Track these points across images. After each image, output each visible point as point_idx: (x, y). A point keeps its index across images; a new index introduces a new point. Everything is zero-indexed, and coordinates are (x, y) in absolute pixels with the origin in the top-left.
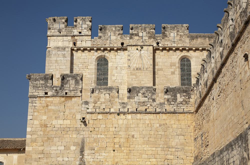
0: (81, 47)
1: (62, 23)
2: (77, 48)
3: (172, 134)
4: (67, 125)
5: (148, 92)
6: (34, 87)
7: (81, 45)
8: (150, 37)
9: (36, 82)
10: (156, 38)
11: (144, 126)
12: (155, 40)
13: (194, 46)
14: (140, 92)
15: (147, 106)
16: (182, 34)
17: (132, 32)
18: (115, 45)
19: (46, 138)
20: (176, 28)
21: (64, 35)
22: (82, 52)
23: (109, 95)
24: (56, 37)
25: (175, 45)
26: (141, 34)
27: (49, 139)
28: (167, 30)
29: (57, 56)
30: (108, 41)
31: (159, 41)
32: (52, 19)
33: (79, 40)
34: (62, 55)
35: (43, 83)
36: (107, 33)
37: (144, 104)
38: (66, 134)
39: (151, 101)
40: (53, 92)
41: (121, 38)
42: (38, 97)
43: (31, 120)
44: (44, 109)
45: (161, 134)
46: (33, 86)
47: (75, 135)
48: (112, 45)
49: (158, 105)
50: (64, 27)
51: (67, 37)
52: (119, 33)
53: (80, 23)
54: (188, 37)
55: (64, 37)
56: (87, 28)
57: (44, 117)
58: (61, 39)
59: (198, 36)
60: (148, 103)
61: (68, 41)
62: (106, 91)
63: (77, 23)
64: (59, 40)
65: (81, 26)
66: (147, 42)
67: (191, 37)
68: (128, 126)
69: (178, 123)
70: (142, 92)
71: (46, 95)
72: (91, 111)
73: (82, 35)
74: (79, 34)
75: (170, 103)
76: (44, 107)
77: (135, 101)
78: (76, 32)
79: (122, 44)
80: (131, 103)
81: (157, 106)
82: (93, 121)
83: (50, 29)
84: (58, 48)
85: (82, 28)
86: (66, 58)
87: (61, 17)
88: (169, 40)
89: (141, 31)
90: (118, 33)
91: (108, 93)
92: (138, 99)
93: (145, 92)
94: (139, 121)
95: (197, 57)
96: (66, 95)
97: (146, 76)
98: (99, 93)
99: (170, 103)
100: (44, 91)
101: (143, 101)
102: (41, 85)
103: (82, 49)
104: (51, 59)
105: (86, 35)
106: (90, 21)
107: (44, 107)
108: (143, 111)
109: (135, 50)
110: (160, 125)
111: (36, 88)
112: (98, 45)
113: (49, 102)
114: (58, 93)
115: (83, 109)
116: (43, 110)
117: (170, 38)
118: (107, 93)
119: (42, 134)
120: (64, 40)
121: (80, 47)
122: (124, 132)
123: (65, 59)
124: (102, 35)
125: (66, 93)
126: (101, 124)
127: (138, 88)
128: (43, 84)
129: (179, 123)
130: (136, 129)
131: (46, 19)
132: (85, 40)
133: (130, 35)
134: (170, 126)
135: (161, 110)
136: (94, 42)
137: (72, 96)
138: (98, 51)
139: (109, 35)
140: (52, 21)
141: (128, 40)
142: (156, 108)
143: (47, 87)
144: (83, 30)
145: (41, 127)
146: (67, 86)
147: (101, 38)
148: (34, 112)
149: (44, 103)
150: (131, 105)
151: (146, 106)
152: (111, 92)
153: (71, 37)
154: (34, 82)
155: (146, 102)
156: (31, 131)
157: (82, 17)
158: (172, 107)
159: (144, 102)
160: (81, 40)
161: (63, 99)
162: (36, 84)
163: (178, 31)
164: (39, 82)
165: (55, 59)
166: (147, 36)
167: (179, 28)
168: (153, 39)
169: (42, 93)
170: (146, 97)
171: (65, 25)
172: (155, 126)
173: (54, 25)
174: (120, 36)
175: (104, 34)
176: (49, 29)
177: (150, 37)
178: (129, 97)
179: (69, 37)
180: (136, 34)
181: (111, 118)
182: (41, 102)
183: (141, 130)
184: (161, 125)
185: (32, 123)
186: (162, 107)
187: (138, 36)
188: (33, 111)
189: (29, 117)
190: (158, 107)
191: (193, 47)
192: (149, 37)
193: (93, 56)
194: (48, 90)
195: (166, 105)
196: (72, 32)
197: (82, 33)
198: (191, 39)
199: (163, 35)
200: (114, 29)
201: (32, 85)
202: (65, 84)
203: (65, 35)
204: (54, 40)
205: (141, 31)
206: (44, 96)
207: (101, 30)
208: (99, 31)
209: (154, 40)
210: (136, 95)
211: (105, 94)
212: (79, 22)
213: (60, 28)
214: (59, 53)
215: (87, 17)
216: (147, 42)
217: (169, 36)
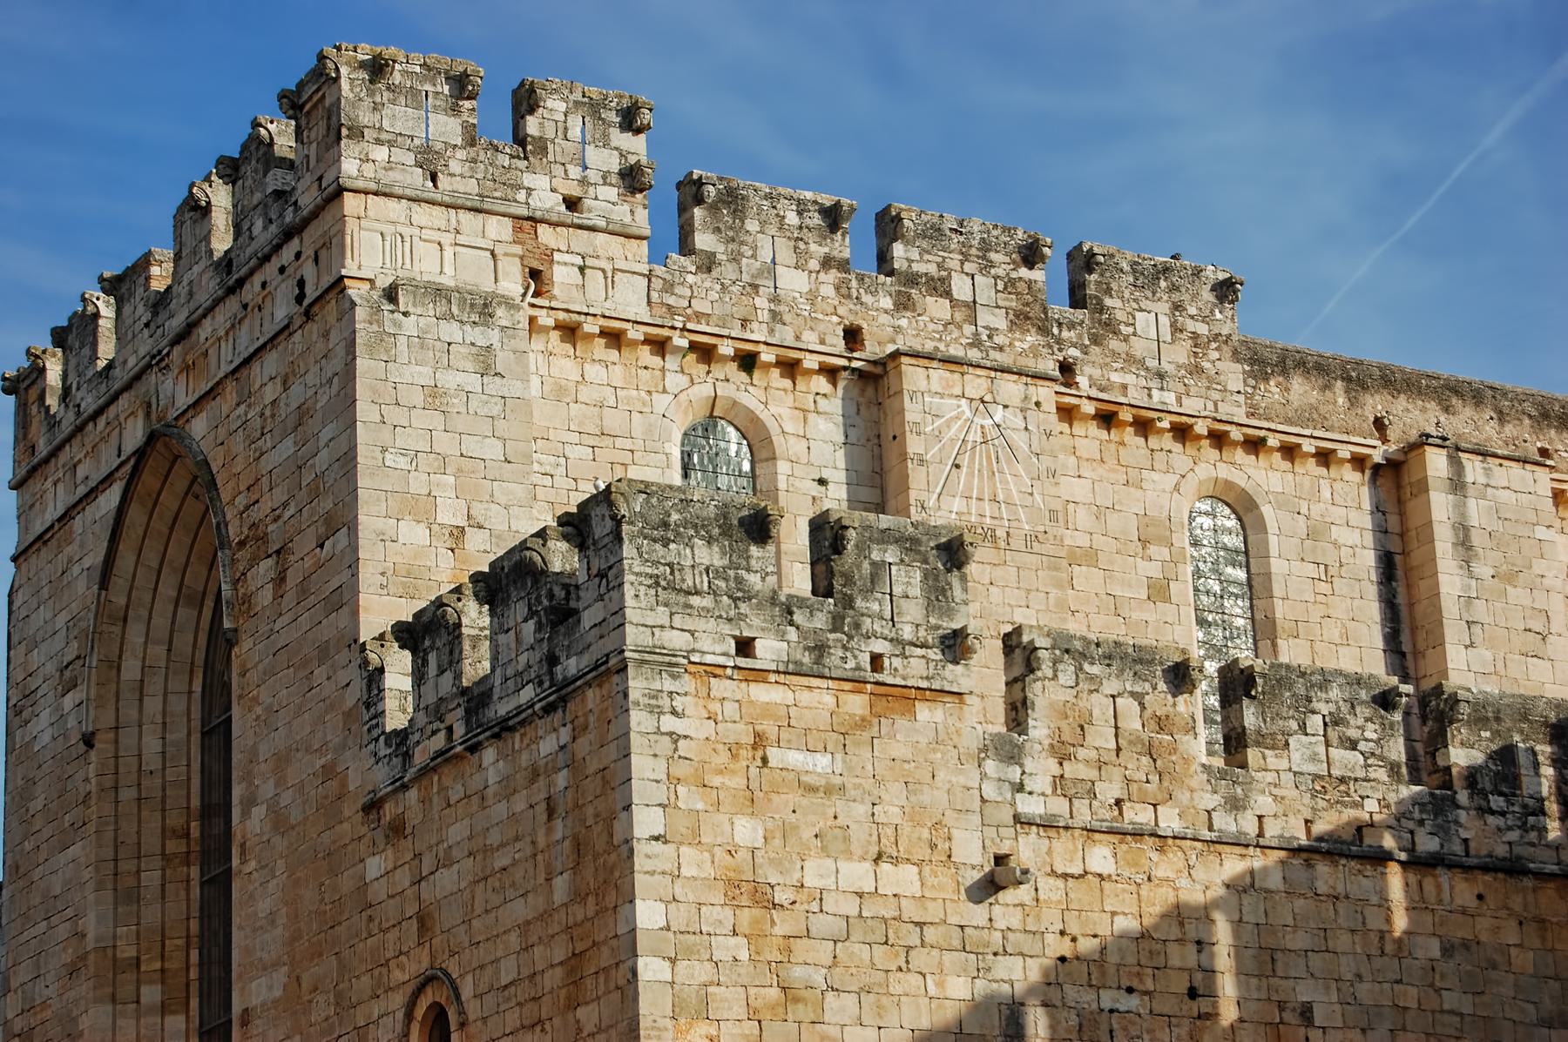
3: (1516, 1016)
4: (904, 902)
5: (1358, 709)
6: (657, 584)
7: (576, 294)
8: (1020, 319)
9: (666, 546)
10: (1055, 331)
11: (1359, 951)
12: (1051, 347)
13: (1273, 426)
14: (1316, 705)
15: (1362, 806)
16: (1202, 329)
17: (910, 261)
18: (804, 338)
19: (774, 993)
20: (1163, 284)
21: (460, 202)
23: (1142, 706)
25: (1170, 398)
26: (961, 288)
27: (796, 1000)
28: (1114, 286)
30: (761, 302)
31: (1075, 359)
34: (474, 351)
35: (718, 562)
36: (750, 239)
37: (1348, 795)
38: (900, 969)
39: (1382, 774)
40: (788, 637)
41: (844, 291)
42: (692, 668)
43: (657, 839)
44: (738, 766)
45: (1455, 1006)
46: (650, 582)
47: (962, 979)
48: (786, 335)
49: (1421, 812)
50: (459, 141)
52: (826, 250)
53: (566, 129)
54: (1236, 356)
55: (465, 216)
57: (747, 831)
59: (1289, 362)
60: (1365, 788)
62: (1117, 676)
66: (1001, 349)
67: (1252, 361)
68: (1270, 942)
69: (1537, 943)
70: (1325, 709)
71: (742, 662)
72: (1042, 811)
74: (563, 208)
75: (1484, 803)
76: (733, 750)
77: (1295, 769)
78: (543, 193)
79: (853, 336)
80: (1270, 777)
81: (1417, 815)
82: (1060, 883)
83: (357, 133)
88: (1131, 360)
89: (962, 264)
90: (818, 250)
91: (1133, 694)
92: (1308, 752)
93: (1345, 708)
94: (1332, 912)
95: (1281, 503)
96: (879, 677)
97: (1029, 591)
98: (1077, 684)
99: (1484, 803)
100: (727, 629)
101: (1336, 772)
105: (617, 228)
107: (733, 750)
108: (1343, 842)
109: (951, 396)
110: (1448, 951)
111: (673, 597)
112: (699, 316)
113: (767, 710)
114: (820, 650)
115: (990, 791)
116: (733, 772)
117: (1139, 347)
118: (1129, 688)
119: (744, 955)
122: (1254, 981)
123: (494, 384)
124: (720, 248)
125: (876, 661)
126: (1114, 914)
127: (1303, 674)
128: (721, 574)
129: (1543, 939)
130: (1316, 961)
133: (900, 283)
134: (1498, 957)
135: (1442, 846)
137: (919, 688)
139: (765, 255)
141: (886, 312)
142: (1411, 825)
143: (750, 599)
144: (591, 189)
145: (732, 902)
146: (876, 607)
147: (714, 273)
148: (673, 780)
149: (738, 719)
150: (1275, 791)
151: (1355, 805)
152: (1147, 686)
153: (508, 222)
154: (658, 546)
155: (1356, 780)
156: (668, 929)
158: (1499, 829)
159: (1342, 780)
161: (857, 704)
162: (670, 565)
163: (1177, 307)
164: (688, 551)
165: (423, 374)
166: (998, 307)
167: (1183, 290)
168: (1039, 337)
169: (715, 645)
170: (1353, 745)
172: (1419, 953)
174: (833, 275)
175: (734, 241)
177: (1020, 319)
178: (1258, 732)
180: (932, 279)
181: (1172, 875)
182: (715, 707)
183: (1347, 969)
184: (1452, 946)
185: (668, 867)
186: (1446, 825)
187: (947, 294)
188: (664, 777)
189: (646, 821)
190: (1421, 823)
191: (1269, 430)
192: (1011, 316)
193: (655, 395)
194: (756, 622)
195: (1463, 814)
196: (519, 187)
197: (590, 211)
198: (1251, 375)
199: (1092, 319)
200: (792, 218)
202: (868, 592)
203: (469, 204)
205: (962, 264)
206: (735, 667)
209: (1041, 340)
210: (1294, 725)
211: (1113, 697)
213: (427, 138)
214: (450, 331)
216: (1001, 349)
217: (1131, 330)
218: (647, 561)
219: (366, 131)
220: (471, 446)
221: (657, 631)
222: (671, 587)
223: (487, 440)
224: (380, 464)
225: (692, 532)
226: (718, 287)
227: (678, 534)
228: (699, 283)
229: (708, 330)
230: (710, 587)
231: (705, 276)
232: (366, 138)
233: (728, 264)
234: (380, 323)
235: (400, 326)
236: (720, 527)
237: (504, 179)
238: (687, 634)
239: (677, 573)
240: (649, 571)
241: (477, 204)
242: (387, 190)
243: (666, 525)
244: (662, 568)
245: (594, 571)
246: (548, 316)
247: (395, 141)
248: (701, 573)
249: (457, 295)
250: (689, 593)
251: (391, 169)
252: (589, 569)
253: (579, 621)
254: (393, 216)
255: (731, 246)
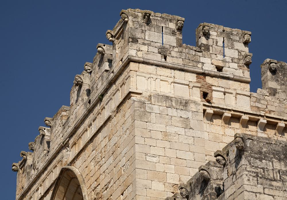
0: (225, 107)
1: (167, 31)
2: (215, 110)
6: (257, 176)
7: (222, 102)
9: (261, 161)
22: (226, 124)
24: (154, 67)
29: (167, 120)
32: (140, 15)
33: (218, 89)
34: (182, 119)
46: (254, 175)
50: (175, 45)
51: (183, 73)
53: (217, 42)
55: (177, 72)
56: (239, 59)
58: (169, 75)
61: (188, 85)
63: (210, 41)
64: (162, 78)
65: (222, 51)
73: (227, 76)
74: (216, 70)
84: (167, 98)
85: (224, 56)
86: (191, 130)
87: (164, 15)
102: (278, 175)
103: (228, 114)
104: (149, 126)
105: (238, 78)
106: (246, 43)
112: (270, 112)
120: (176, 80)
121: (223, 109)
124: (278, 87)
131: (123, 11)
132: (234, 92)
136: (258, 100)
138: (267, 130)
140: (140, 19)
144: (227, 64)
147: (277, 96)
153: (195, 75)
154: (257, 161)
157: (222, 28)
160: (223, 90)
164: (270, 163)
165: (162, 127)
171: (178, 40)
173: (147, 33)
175: (284, 84)
176: (132, 42)
179: (189, 74)
196: (199, 62)
201: (251, 169)
204: (149, 76)
207: (274, 72)
208: (269, 74)
212: (215, 37)
213: (163, 43)
214: (172, 112)
215: (235, 31)
218: (253, 166)
219: (139, 40)
220: (180, 154)
221: (258, 195)
222: (262, 177)
223: (188, 152)
224: (145, 160)
225: (272, 156)
226: (278, 101)
227: (265, 156)
228: (270, 99)
229: (275, 116)
230: (280, 178)
231: (273, 97)
232: (139, 42)
233: (282, 93)
234: (145, 108)
235: (152, 109)
236: (284, 154)
237: (193, 59)
238: (271, 197)
239: (266, 172)
240: (254, 170)
241: (183, 67)
242: (148, 61)
243: (260, 153)
244: (259, 170)
245: (230, 173)
246: (211, 109)
247: (150, 44)
248: (276, 172)
249: (175, 99)
250: (271, 180)
251: (149, 54)
252: (228, 173)
253: (224, 195)
254: (150, 71)
255: (282, 87)
